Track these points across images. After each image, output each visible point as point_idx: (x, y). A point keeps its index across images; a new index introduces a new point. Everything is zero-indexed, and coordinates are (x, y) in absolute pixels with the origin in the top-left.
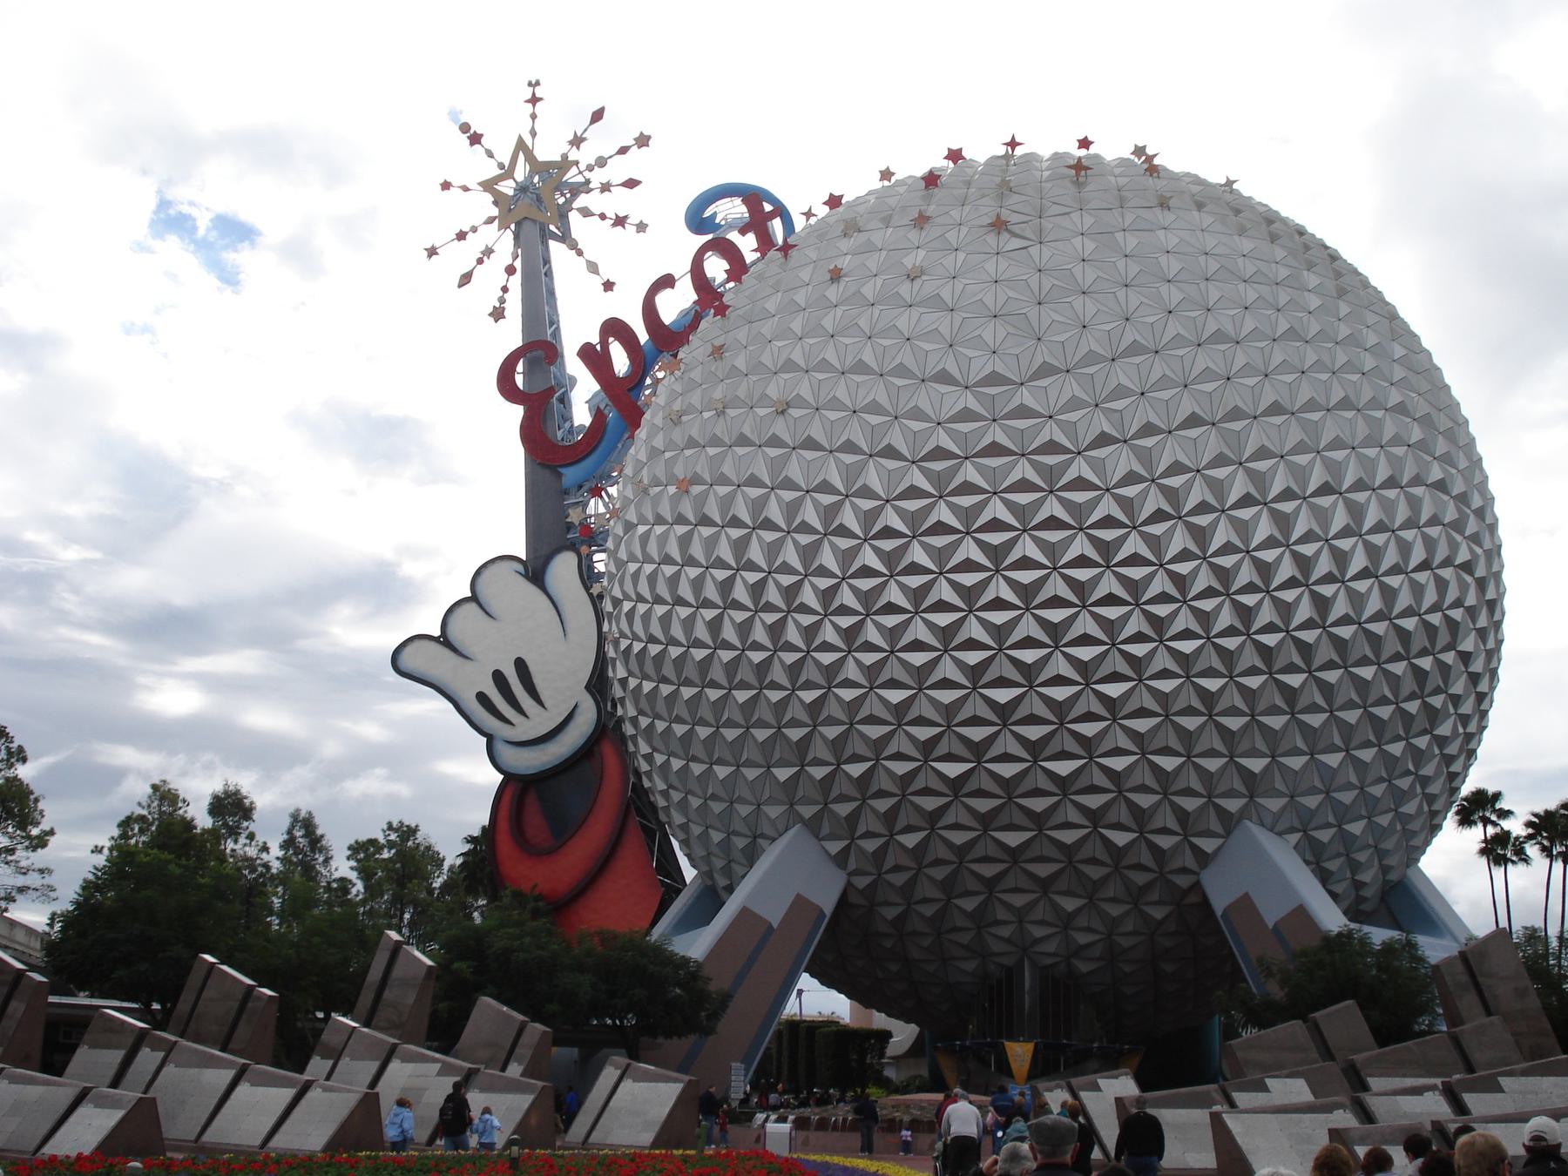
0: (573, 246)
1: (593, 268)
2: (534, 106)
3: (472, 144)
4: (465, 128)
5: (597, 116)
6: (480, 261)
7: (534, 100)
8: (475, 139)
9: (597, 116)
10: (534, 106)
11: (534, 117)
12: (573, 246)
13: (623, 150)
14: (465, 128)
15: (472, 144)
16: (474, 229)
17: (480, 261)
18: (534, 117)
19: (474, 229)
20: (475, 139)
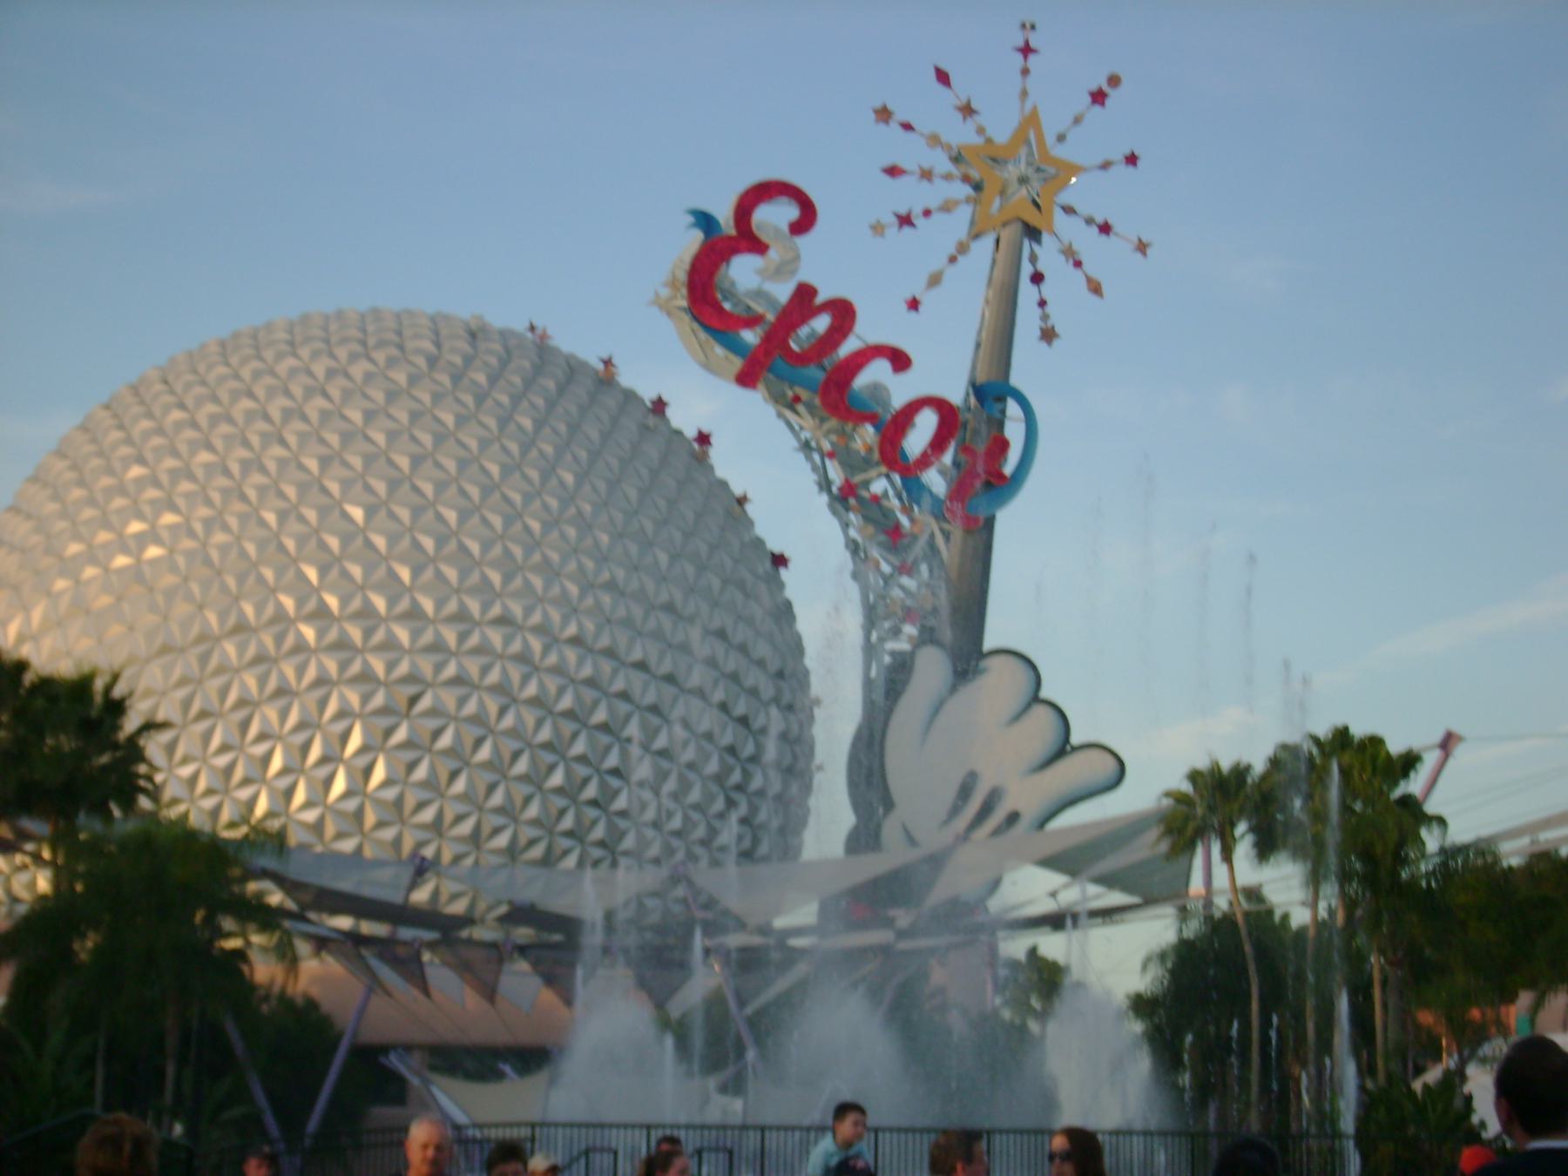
0: (963, 248)
1: (935, 280)
2: (1026, 57)
3: (1102, 104)
4: (1114, 81)
5: (943, 77)
6: (1078, 264)
7: (1026, 50)
8: (1099, 97)
9: (943, 77)
10: (1026, 57)
11: (1025, 72)
12: (963, 248)
13: (907, 127)
14: (1114, 81)
15: (1102, 104)
16: (1089, 221)
17: (1078, 264)
18: (1025, 72)
19: (1089, 221)
20: (1099, 97)
